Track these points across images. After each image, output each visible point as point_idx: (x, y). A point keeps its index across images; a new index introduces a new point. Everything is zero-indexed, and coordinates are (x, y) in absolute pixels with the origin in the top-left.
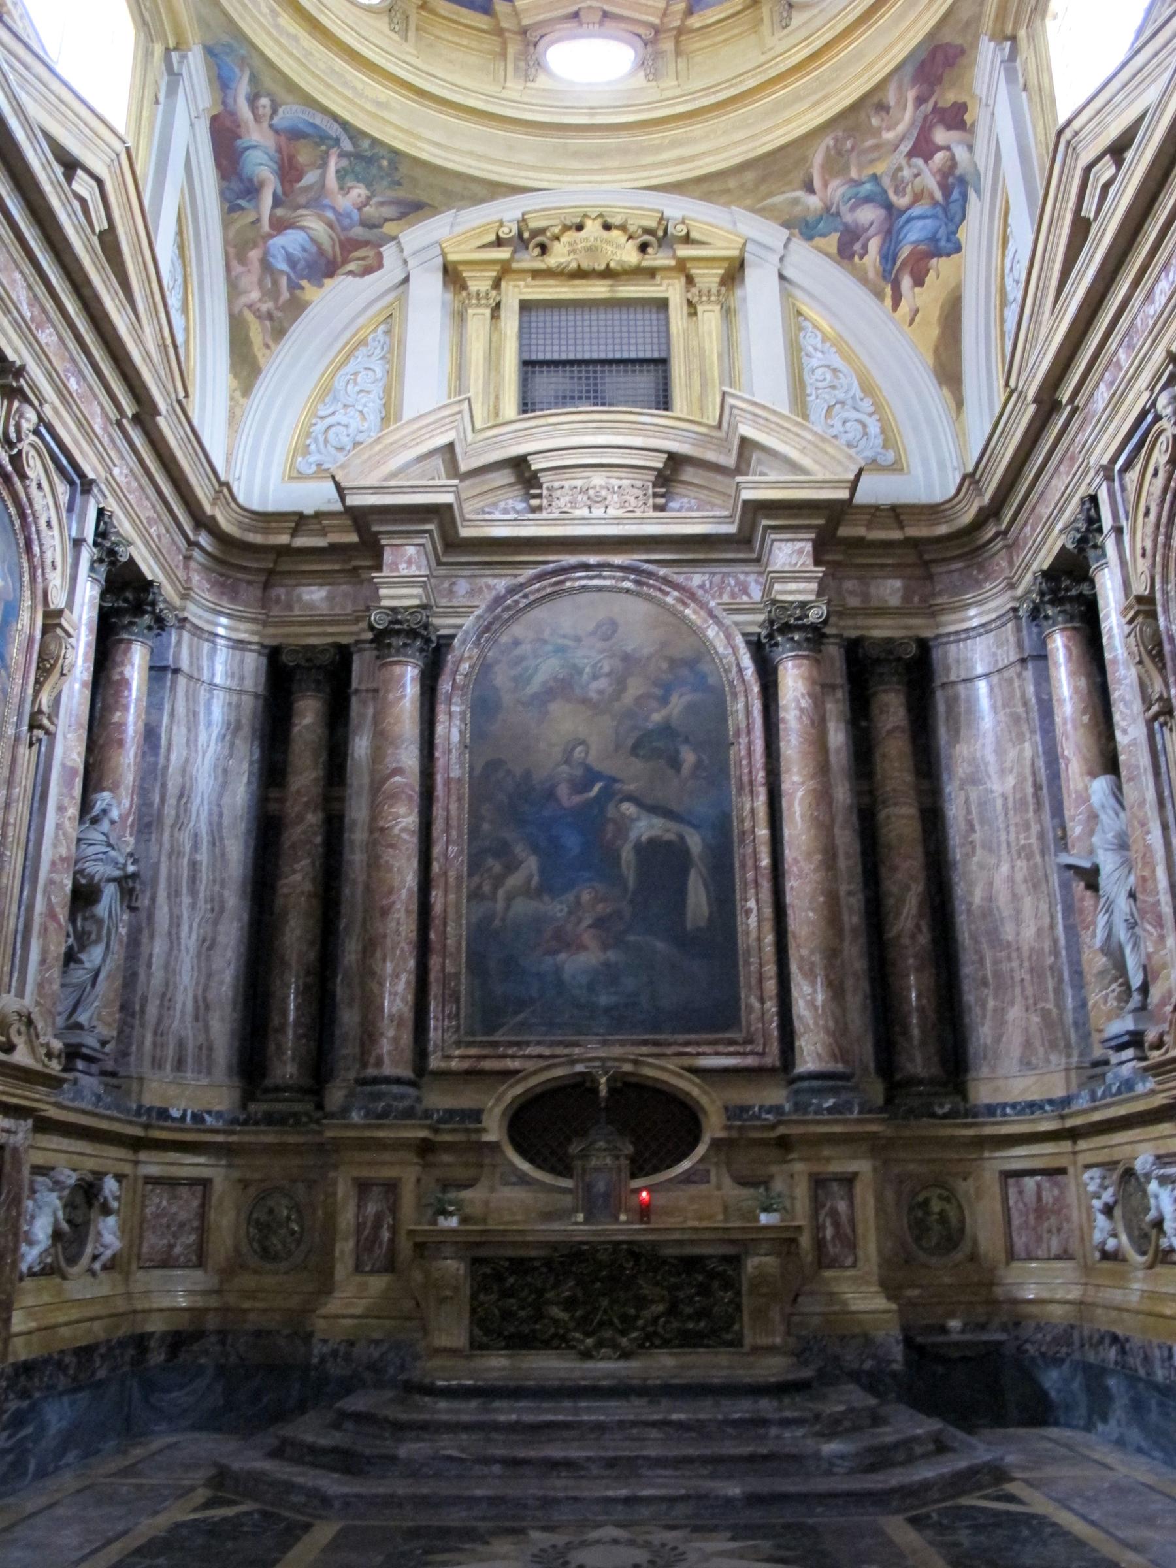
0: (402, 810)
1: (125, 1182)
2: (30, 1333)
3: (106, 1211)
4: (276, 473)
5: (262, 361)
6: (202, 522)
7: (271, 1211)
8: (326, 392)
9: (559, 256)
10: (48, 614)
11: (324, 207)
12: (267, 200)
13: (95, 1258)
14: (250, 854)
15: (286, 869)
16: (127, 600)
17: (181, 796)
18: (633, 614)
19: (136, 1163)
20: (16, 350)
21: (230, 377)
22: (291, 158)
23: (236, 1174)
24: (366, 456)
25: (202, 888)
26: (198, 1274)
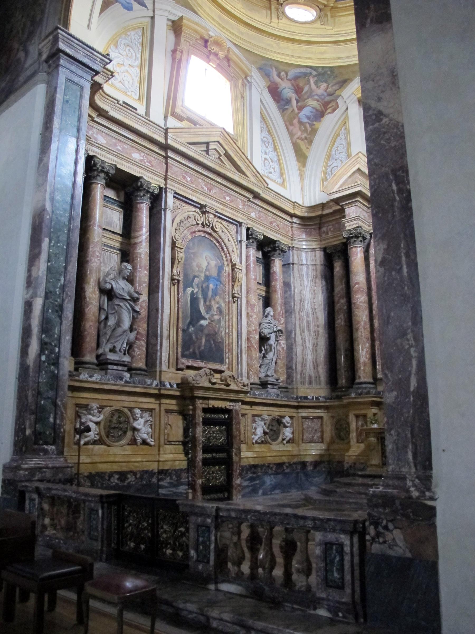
0: (359, 296)
1: (294, 419)
2: (254, 457)
3: (286, 427)
4: (318, 189)
5: (307, 154)
6: (292, 216)
7: (341, 425)
8: (329, 157)
10: (232, 266)
11: (313, 96)
12: (294, 102)
13: (284, 440)
14: (326, 315)
15: (336, 319)
16: (267, 249)
17: (301, 302)
19: (298, 413)
20: (203, 200)
21: (297, 163)
22: (298, 86)
23: (330, 414)
24: (332, 182)
25: (311, 329)
26: (322, 445)
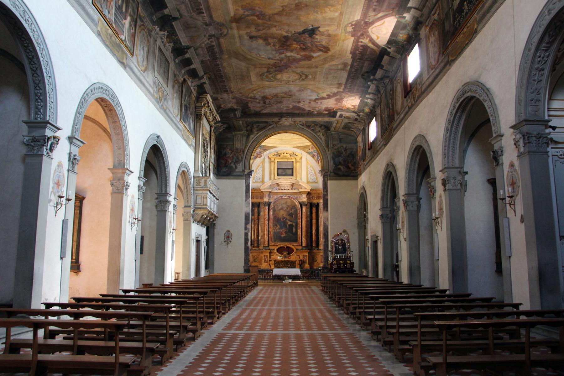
9: (281, 156)
18: (289, 200)
